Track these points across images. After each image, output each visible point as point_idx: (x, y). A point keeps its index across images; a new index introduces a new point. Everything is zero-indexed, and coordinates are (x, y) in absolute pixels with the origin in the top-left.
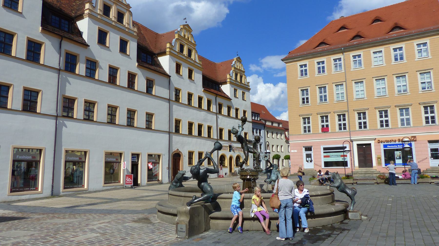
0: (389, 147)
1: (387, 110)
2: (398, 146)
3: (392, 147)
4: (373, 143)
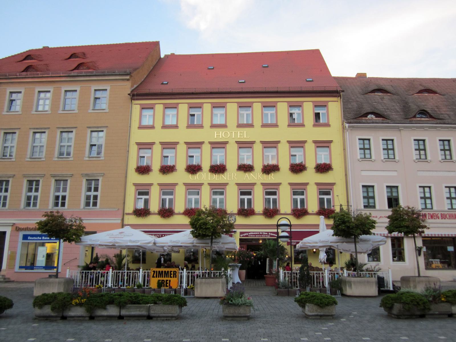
0: (30, 240)
1: (39, 181)
2: (43, 238)
3: (34, 240)
4: (9, 231)
